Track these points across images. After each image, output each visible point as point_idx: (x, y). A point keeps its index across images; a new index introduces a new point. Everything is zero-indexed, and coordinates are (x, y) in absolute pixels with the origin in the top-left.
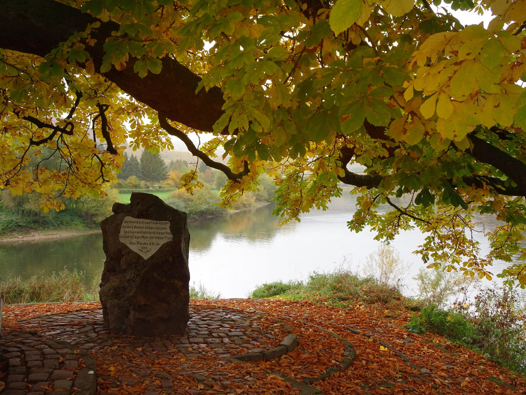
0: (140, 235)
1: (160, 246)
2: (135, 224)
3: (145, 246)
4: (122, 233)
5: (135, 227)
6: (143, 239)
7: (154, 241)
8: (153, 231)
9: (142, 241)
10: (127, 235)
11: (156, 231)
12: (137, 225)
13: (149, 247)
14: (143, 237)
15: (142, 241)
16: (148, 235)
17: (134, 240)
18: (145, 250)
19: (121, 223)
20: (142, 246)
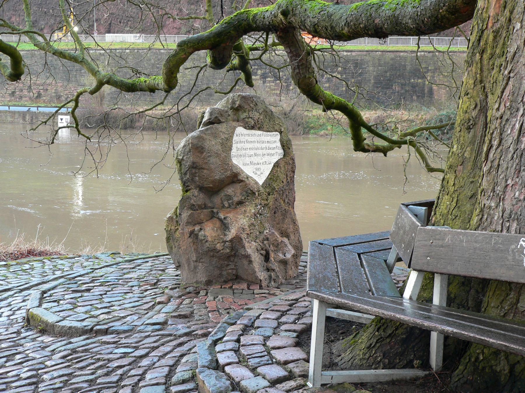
0: (252, 152)
1: (273, 164)
2: (247, 138)
3: (258, 166)
4: (234, 152)
5: (248, 142)
6: (256, 157)
7: (266, 158)
8: (264, 145)
9: (255, 160)
10: (240, 153)
11: (267, 145)
12: (250, 139)
13: (262, 167)
14: (256, 155)
15: (255, 160)
16: (260, 152)
17: (248, 160)
18: (259, 173)
19: (232, 137)
20: (256, 166)
